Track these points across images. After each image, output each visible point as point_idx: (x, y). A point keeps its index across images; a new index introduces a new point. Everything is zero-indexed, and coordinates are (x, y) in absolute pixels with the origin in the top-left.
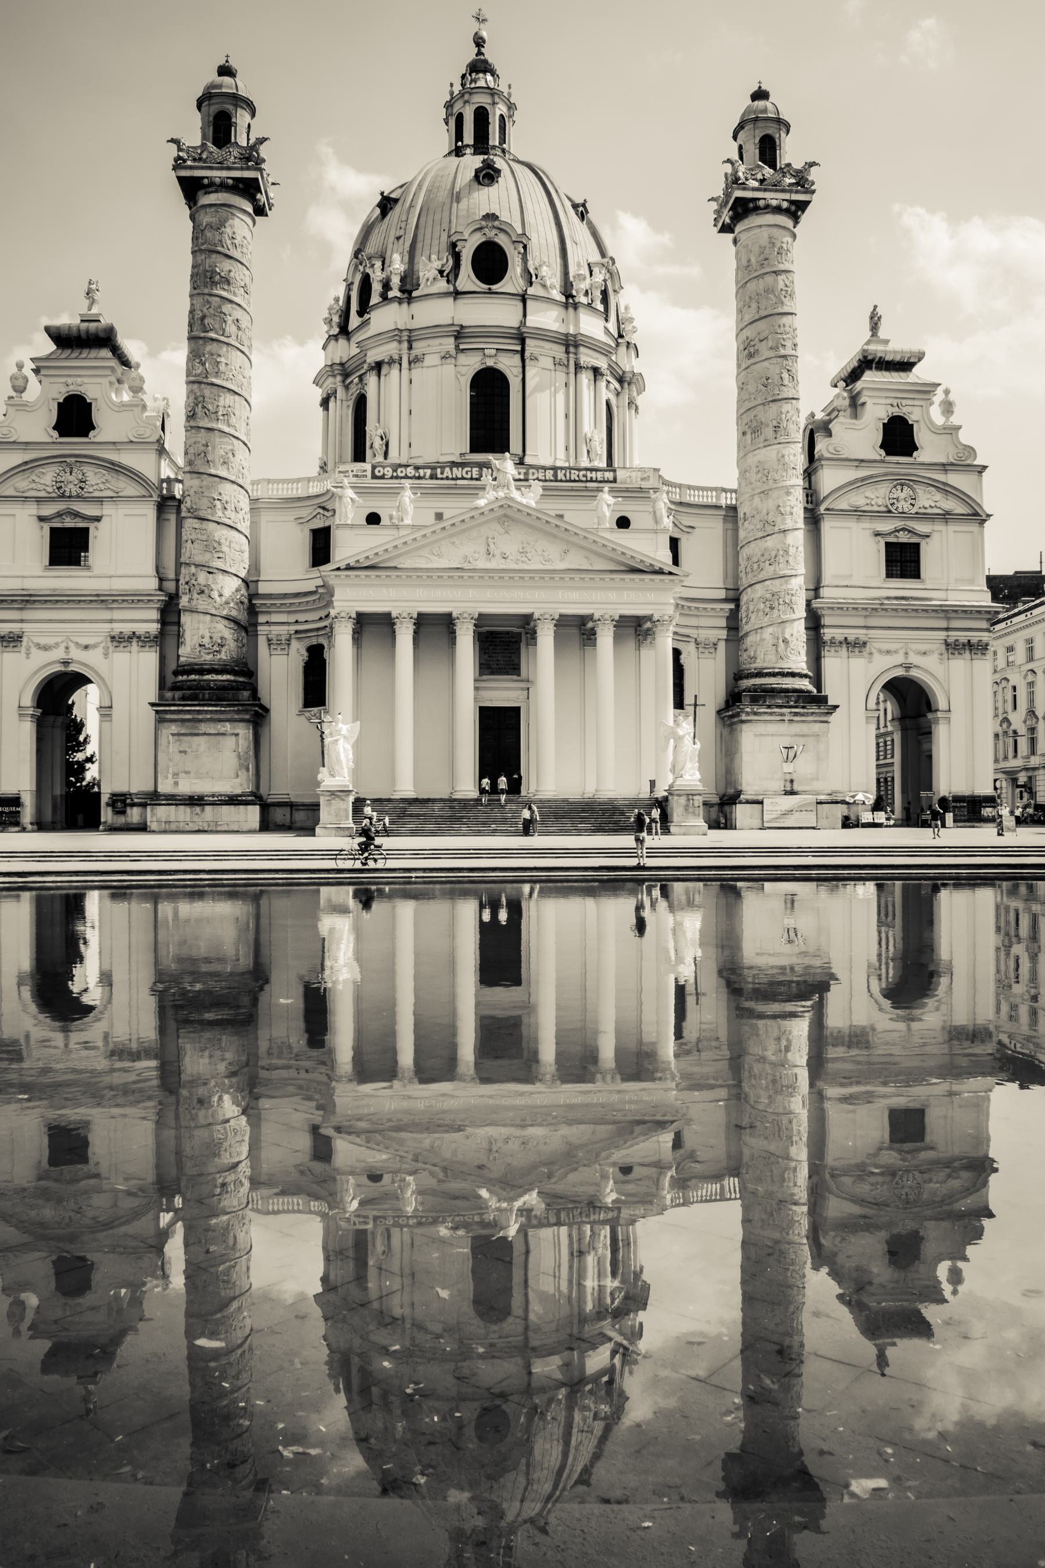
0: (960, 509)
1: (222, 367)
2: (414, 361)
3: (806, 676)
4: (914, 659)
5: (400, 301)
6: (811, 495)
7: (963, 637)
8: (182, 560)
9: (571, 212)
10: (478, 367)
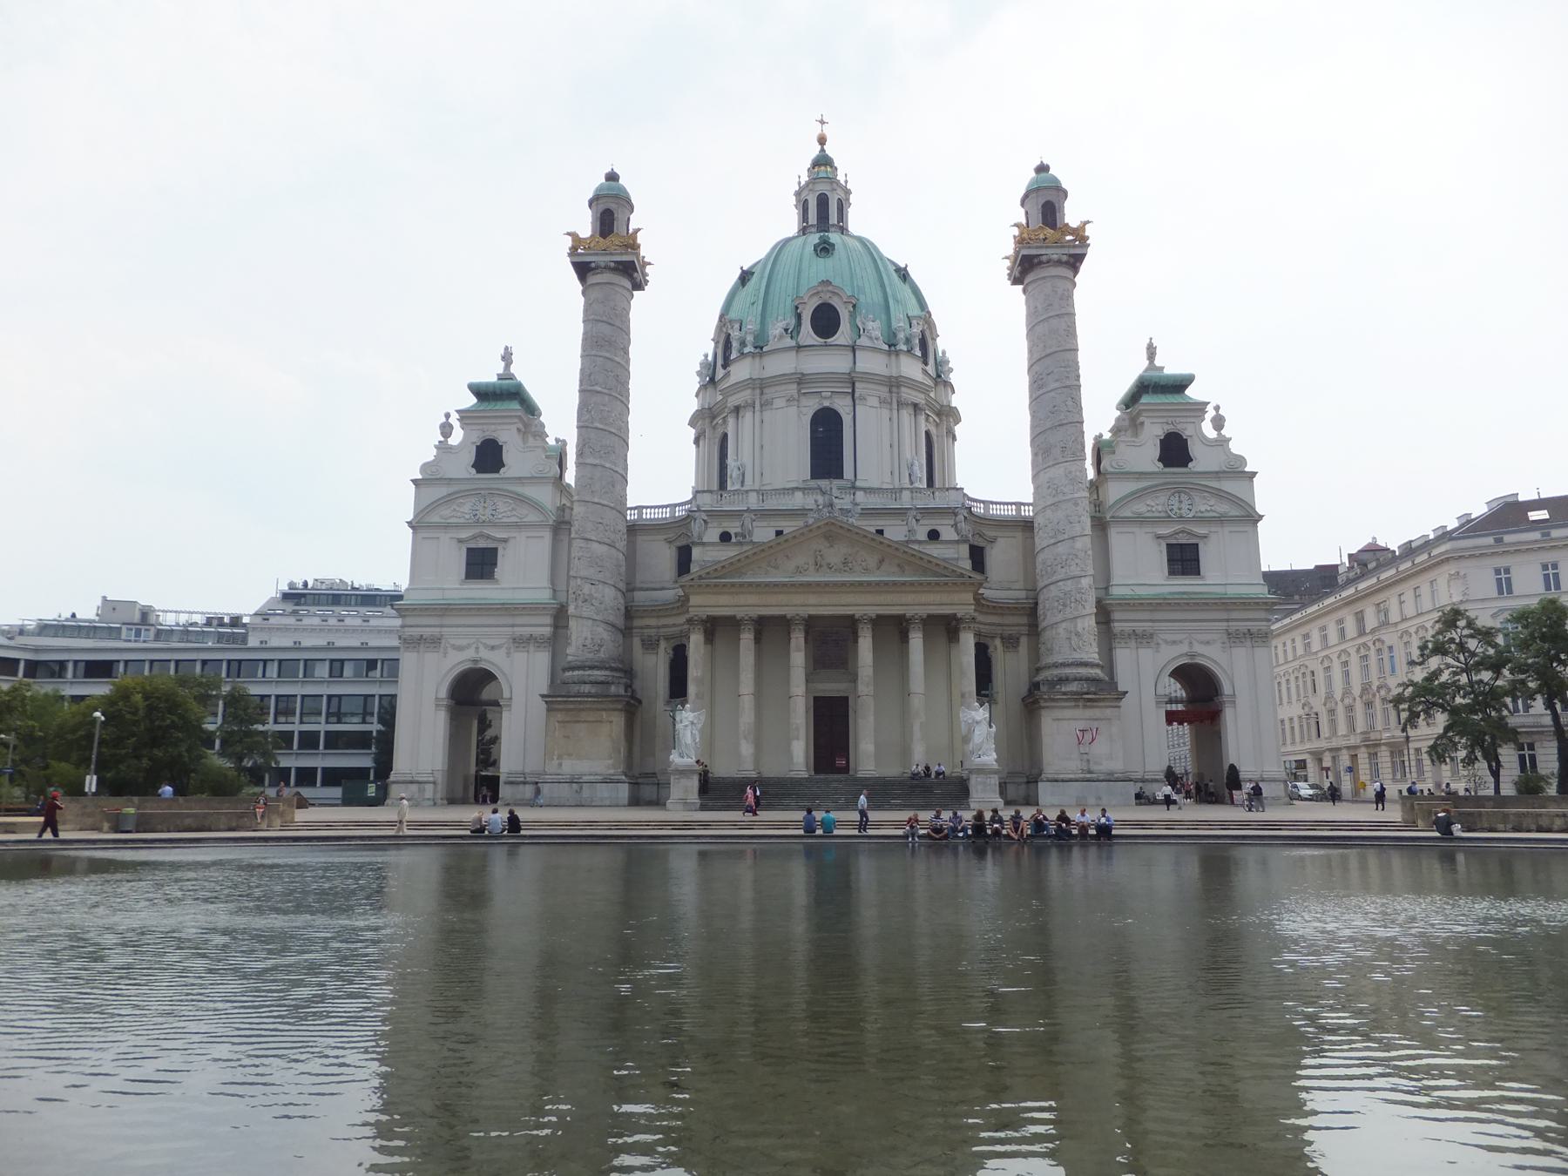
0: (1235, 512)
2: (766, 404)
3: (1097, 665)
4: (1198, 648)
5: (753, 355)
6: (1098, 505)
7: (1243, 626)
8: (572, 573)
9: (895, 275)
10: (817, 407)
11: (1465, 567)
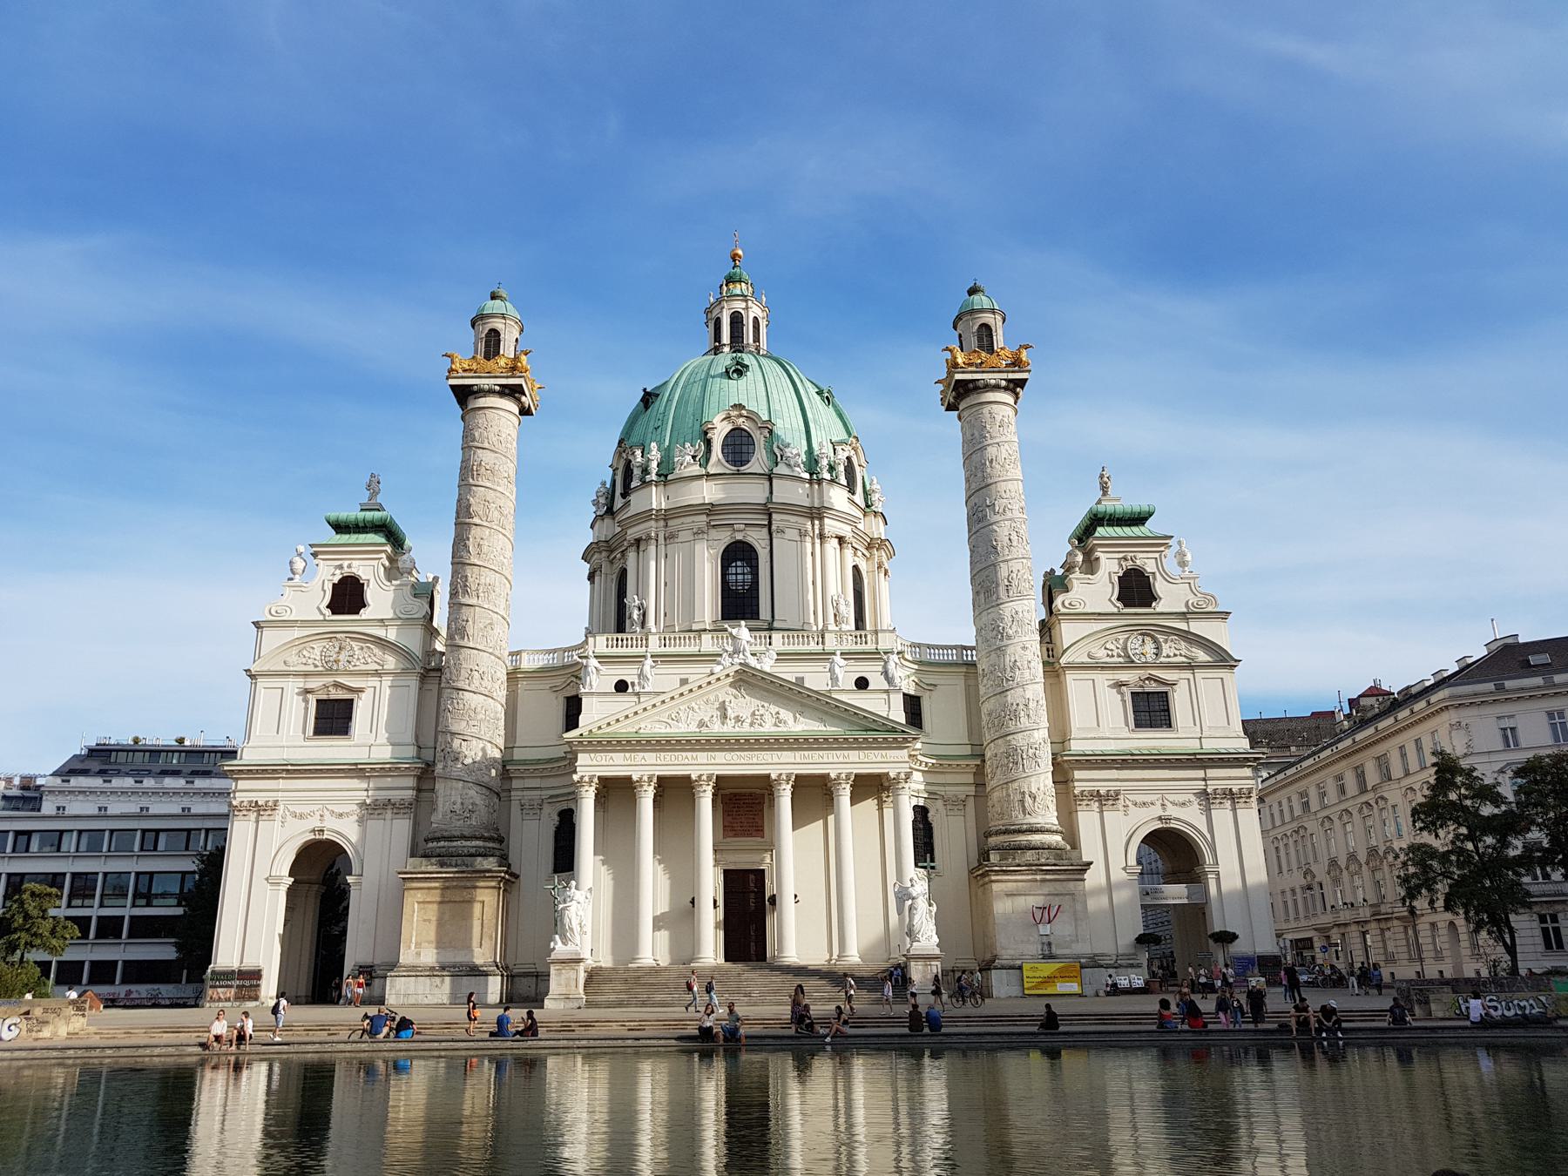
1: (485, 549)
11: (1467, 715)
